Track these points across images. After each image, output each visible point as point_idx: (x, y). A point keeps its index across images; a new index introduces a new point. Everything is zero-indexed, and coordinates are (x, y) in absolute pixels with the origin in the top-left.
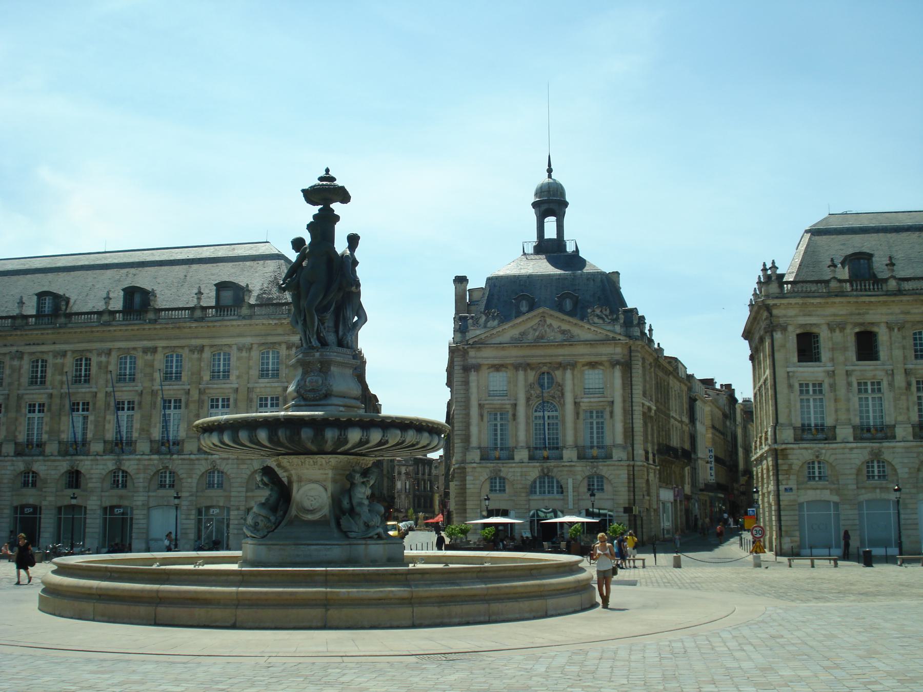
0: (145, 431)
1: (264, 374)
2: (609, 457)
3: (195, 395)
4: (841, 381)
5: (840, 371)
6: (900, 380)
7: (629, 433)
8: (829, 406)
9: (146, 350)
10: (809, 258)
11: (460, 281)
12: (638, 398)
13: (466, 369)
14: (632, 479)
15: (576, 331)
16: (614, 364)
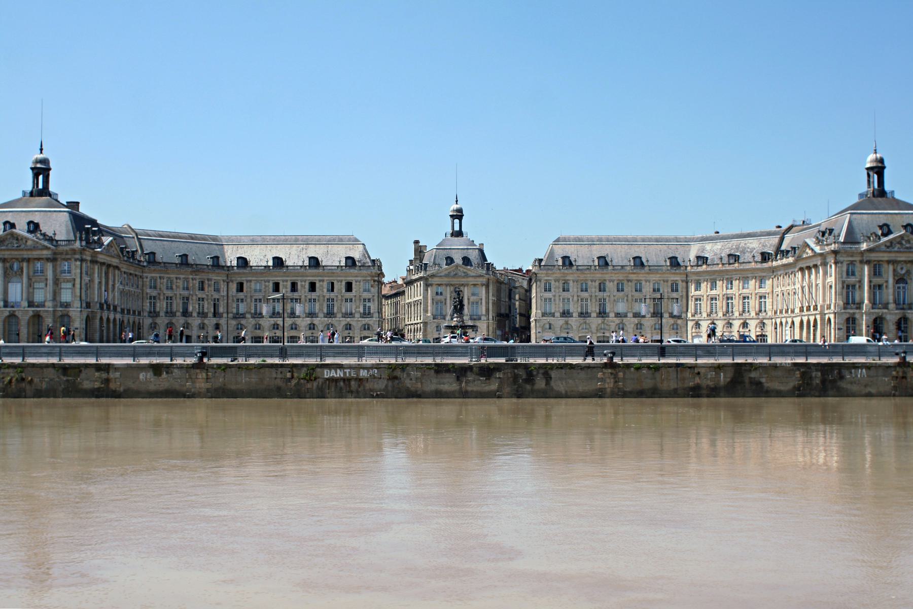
0: (321, 310)
1: (365, 291)
2: (480, 319)
3: (340, 297)
4: (557, 298)
5: (557, 295)
6: (575, 298)
7: (487, 310)
8: (553, 306)
9: (320, 281)
10: (551, 254)
11: (417, 242)
12: (491, 297)
13: (427, 285)
14: (488, 327)
15: (469, 272)
16: (482, 285)
